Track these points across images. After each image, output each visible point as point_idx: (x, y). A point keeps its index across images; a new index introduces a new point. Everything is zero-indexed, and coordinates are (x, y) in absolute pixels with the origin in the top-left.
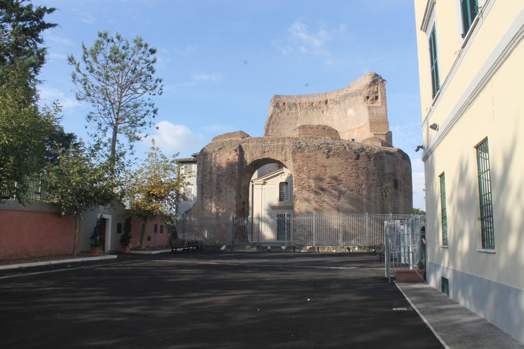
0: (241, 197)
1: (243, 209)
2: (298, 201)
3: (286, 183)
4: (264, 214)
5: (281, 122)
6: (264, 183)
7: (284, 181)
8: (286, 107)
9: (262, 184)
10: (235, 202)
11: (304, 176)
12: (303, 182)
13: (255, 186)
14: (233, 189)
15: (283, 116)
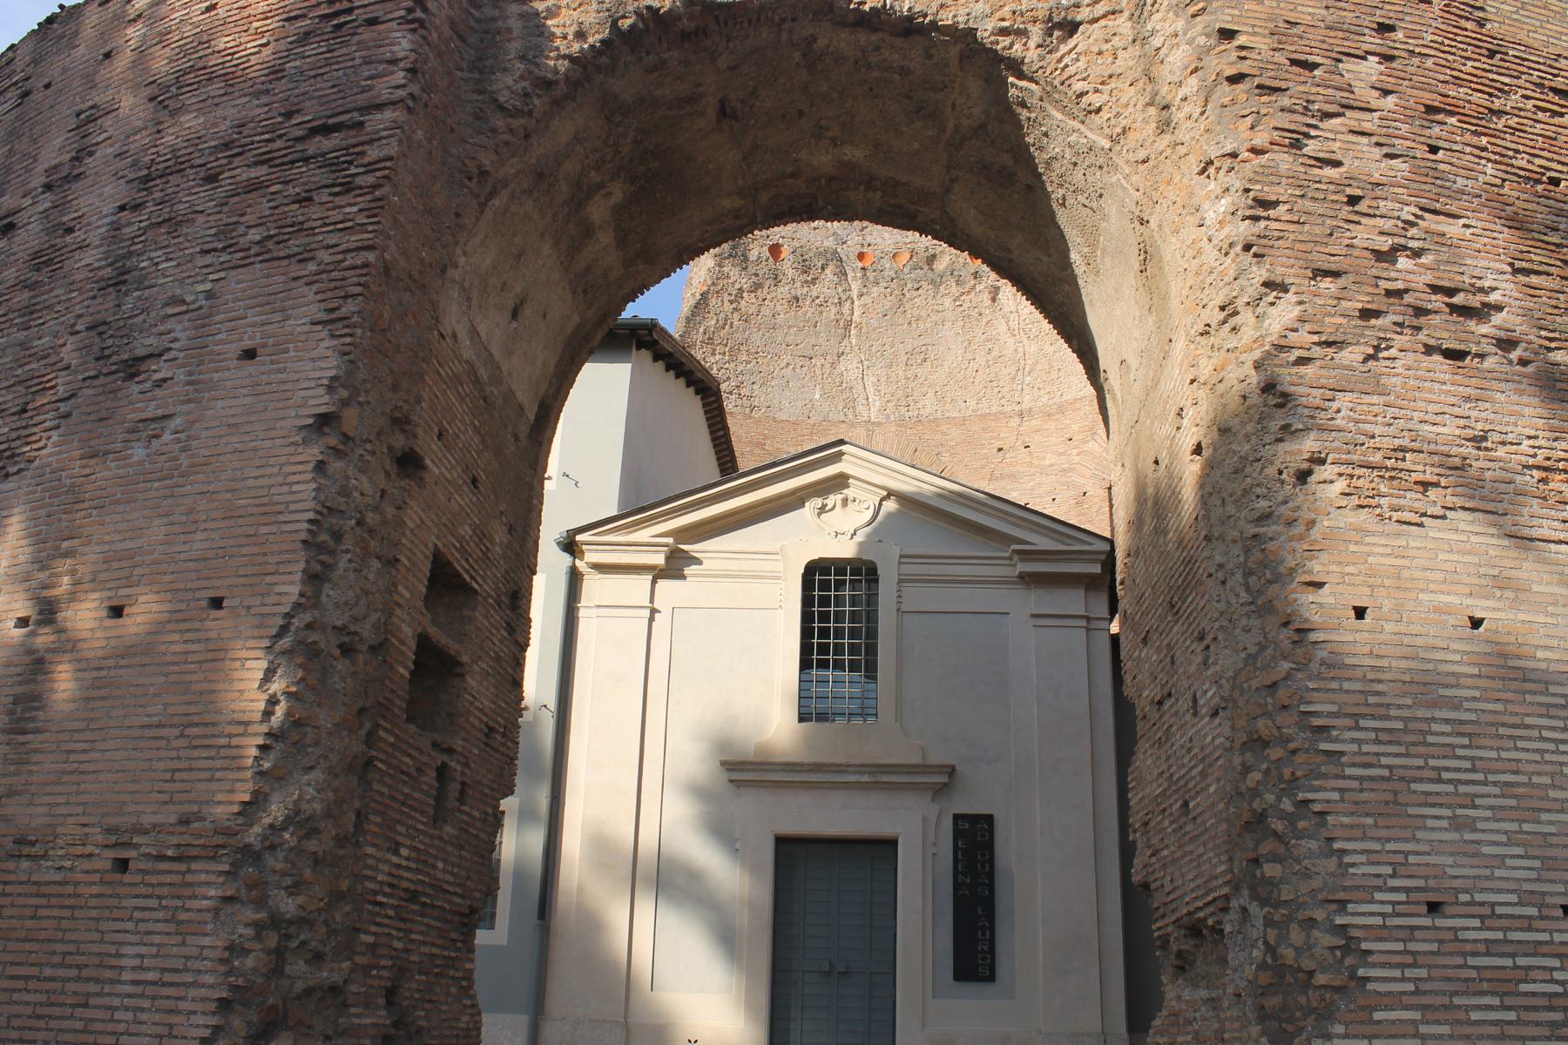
0: (409, 463)
1: (435, 666)
2: (1330, 486)
3: (863, 572)
4: (672, 823)
5: (757, 338)
6: (675, 565)
7: (845, 550)
8: (788, 266)
9: (659, 574)
10: (304, 493)
11: (1365, 161)
12: (1368, 235)
13: (595, 588)
14: (308, 305)
15: (766, 311)
